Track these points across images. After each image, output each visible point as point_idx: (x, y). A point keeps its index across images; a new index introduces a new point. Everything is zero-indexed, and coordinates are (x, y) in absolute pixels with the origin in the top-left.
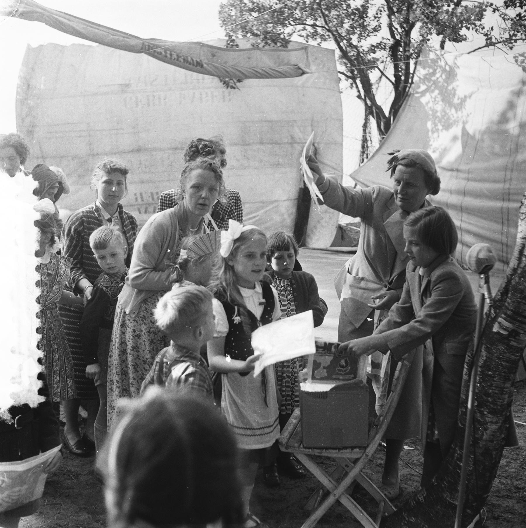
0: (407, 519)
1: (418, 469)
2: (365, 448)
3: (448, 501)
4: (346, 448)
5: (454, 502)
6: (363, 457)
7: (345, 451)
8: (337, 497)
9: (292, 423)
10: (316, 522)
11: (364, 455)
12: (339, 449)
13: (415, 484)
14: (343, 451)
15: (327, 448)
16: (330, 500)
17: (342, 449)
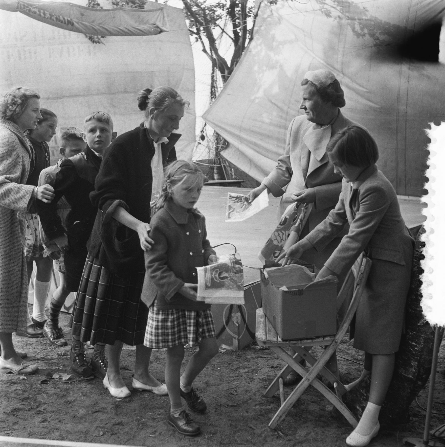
0: (365, 395)
1: (340, 355)
2: (335, 336)
3: (404, 376)
4: (318, 337)
5: (409, 376)
6: (332, 344)
7: (318, 340)
8: (310, 381)
9: (260, 321)
10: (292, 405)
11: (334, 342)
12: (312, 339)
13: (345, 367)
14: (316, 340)
15: (301, 339)
16: (302, 385)
17: (315, 339)
